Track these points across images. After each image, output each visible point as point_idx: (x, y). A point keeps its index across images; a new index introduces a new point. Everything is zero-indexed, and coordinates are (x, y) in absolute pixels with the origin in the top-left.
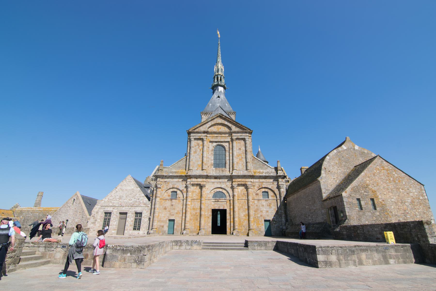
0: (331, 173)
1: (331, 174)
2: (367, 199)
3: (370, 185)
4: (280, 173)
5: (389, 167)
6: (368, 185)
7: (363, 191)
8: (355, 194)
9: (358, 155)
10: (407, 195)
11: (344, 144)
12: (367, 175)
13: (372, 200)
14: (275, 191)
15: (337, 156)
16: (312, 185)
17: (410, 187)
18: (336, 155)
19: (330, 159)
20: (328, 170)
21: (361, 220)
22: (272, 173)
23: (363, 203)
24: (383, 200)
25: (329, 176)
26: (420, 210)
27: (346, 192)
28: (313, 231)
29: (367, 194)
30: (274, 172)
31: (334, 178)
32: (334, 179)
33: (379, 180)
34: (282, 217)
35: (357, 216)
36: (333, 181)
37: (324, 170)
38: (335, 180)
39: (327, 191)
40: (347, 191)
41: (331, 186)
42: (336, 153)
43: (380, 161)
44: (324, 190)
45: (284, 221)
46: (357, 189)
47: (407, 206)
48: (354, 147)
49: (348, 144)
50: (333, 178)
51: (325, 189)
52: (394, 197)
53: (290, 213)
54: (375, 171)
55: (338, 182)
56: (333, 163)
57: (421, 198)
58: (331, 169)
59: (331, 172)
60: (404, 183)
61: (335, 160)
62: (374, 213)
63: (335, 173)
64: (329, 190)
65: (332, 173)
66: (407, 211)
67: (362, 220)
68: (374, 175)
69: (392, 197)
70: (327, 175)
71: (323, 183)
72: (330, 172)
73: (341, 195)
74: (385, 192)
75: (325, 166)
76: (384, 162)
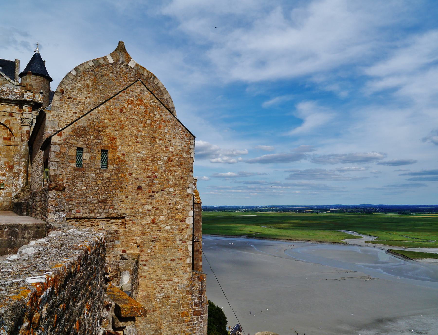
0: (73, 101)
1: (71, 103)
2: (96, 151)
3: (110, 127)
4: (27, 97)
5: (151, 101)
7: (92, 137)
8: (76, 140)
9: (130, 78)
10: (165, 149)
12: (109, 110)
14: (13, 129)
15: (92, 72)
17: (174, 138)
18: (90, 70)
19: (77, 75)
20: (68, 96)
21: (75, 183)
22: (11, 95)
23: (86, 156)
24: (123, 155)
25: (66, 107)
26: (176, 174)
29: (99, 141)
30: (17, 93)
31: (76, 112)
32: (76, 113)
34: (18, 177)
35: (69, 176)
36: (72, 116)
40: (63, 134)
42: (93, 66)
43: (139, 89)
44: (50, 131)
46: (83, 132)
47: (160, 166)
48: (128, 63)
49: (119, 55)
50: (73, 111)
52: (143, 151)
54: (126, 105)
56: (80, 84)
57: (185, 156)
58: (74, 95)
60: (166, 130)
61: (85, 80)
62: (101, 174)
63: (80, 102)
65: (75, 102)
66: (156, 174)
67: (77, 185)
68: (121, 111)
69: (139, 150)
72: (70, 100)
74: (130, 141)
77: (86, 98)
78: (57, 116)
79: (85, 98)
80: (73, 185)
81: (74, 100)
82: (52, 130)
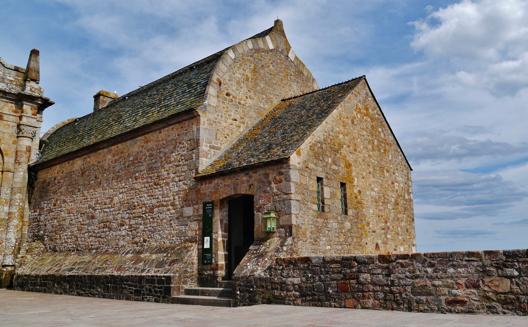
0: (232, 101)
4: (31, 90)
6: (341, 146)
7: (330, 160)
11: (271, 34)
13: (343, 185)
15: (252, 59)
16: (165, 127)
19: (235, 59)
20: (226, 91)
21: (319, 240)
25: (224, 108)
27: (299, 154)
28: (144, 274)
30: (11, 81)
32: (236, 120)
33: (358, 137)
37: (216, 86)
38: (237, 122)
39: (213, 150)
41: (226, 137)
44: (206, 146)
45: (14, 241)
46: (320, 150)
49: (278, 39)
50: (232, 117)
51: (208, 145)
53: (40, 215)
55: (241, 130)
58: (233, 91)
59: (231, 96)
64: (218, 149)
65: (234, 103)
70: (221, 104)
71: (206, 123)
73: (288, 159)
75: (220, 74)
76: (370, 99)
77: (247, 97)
78: (214, 122)
79: (245, 98)
80: (317, 243)
81: (234, 99)
82: (208, 145)
